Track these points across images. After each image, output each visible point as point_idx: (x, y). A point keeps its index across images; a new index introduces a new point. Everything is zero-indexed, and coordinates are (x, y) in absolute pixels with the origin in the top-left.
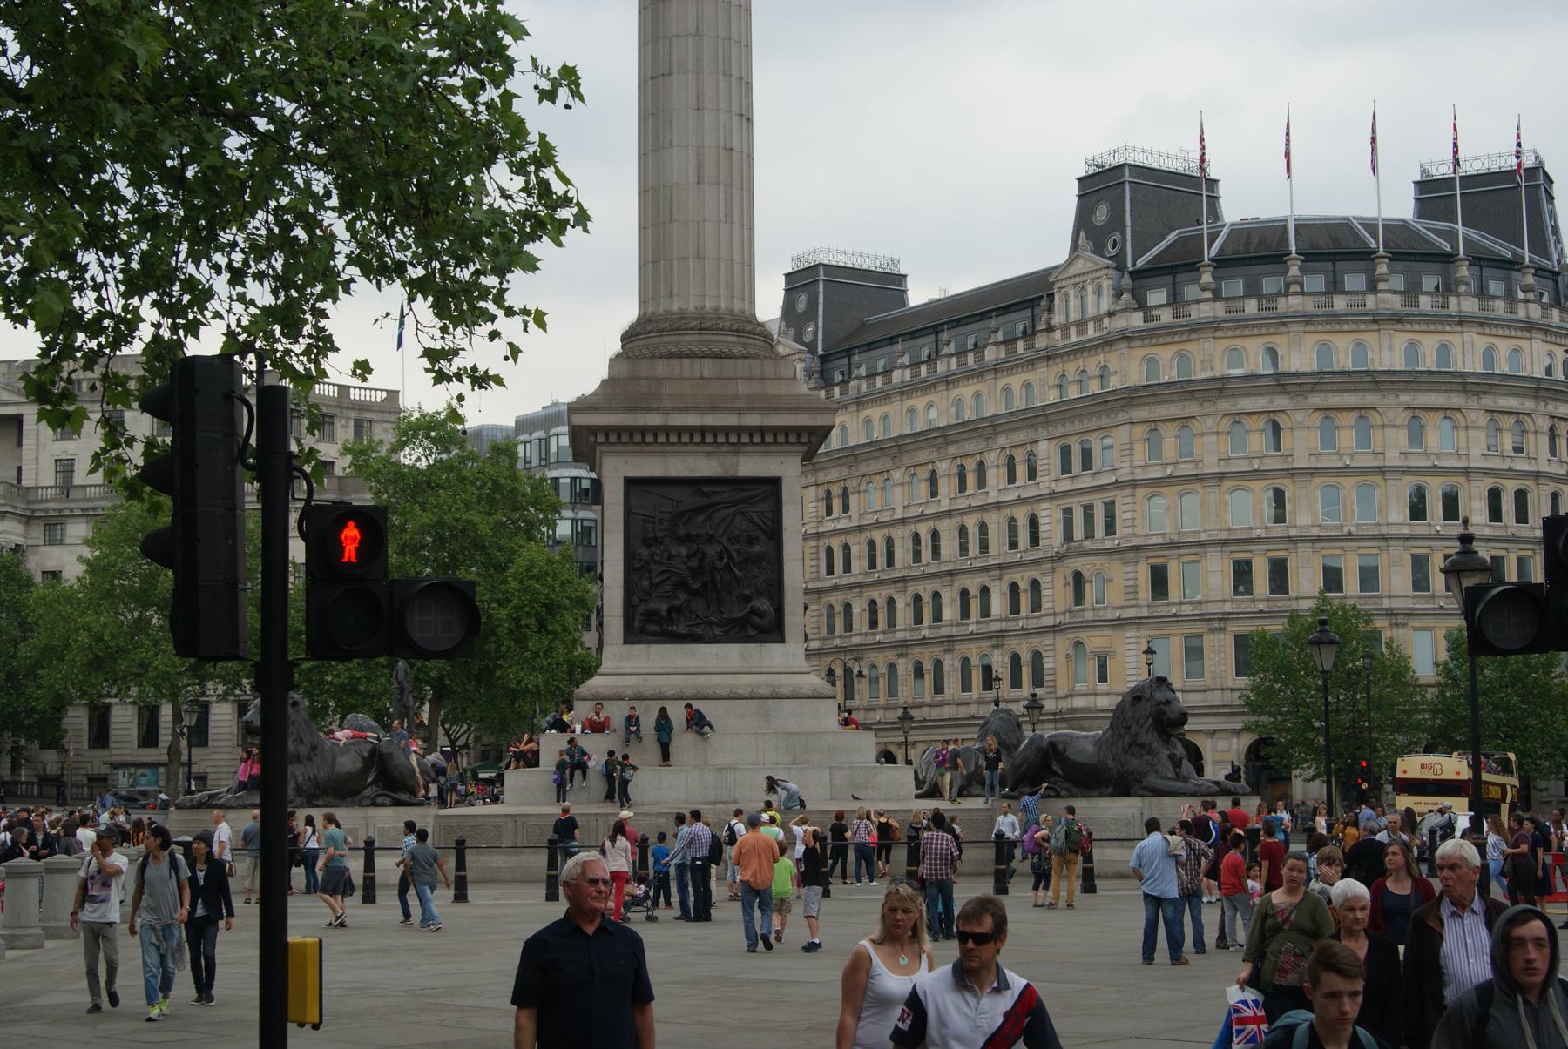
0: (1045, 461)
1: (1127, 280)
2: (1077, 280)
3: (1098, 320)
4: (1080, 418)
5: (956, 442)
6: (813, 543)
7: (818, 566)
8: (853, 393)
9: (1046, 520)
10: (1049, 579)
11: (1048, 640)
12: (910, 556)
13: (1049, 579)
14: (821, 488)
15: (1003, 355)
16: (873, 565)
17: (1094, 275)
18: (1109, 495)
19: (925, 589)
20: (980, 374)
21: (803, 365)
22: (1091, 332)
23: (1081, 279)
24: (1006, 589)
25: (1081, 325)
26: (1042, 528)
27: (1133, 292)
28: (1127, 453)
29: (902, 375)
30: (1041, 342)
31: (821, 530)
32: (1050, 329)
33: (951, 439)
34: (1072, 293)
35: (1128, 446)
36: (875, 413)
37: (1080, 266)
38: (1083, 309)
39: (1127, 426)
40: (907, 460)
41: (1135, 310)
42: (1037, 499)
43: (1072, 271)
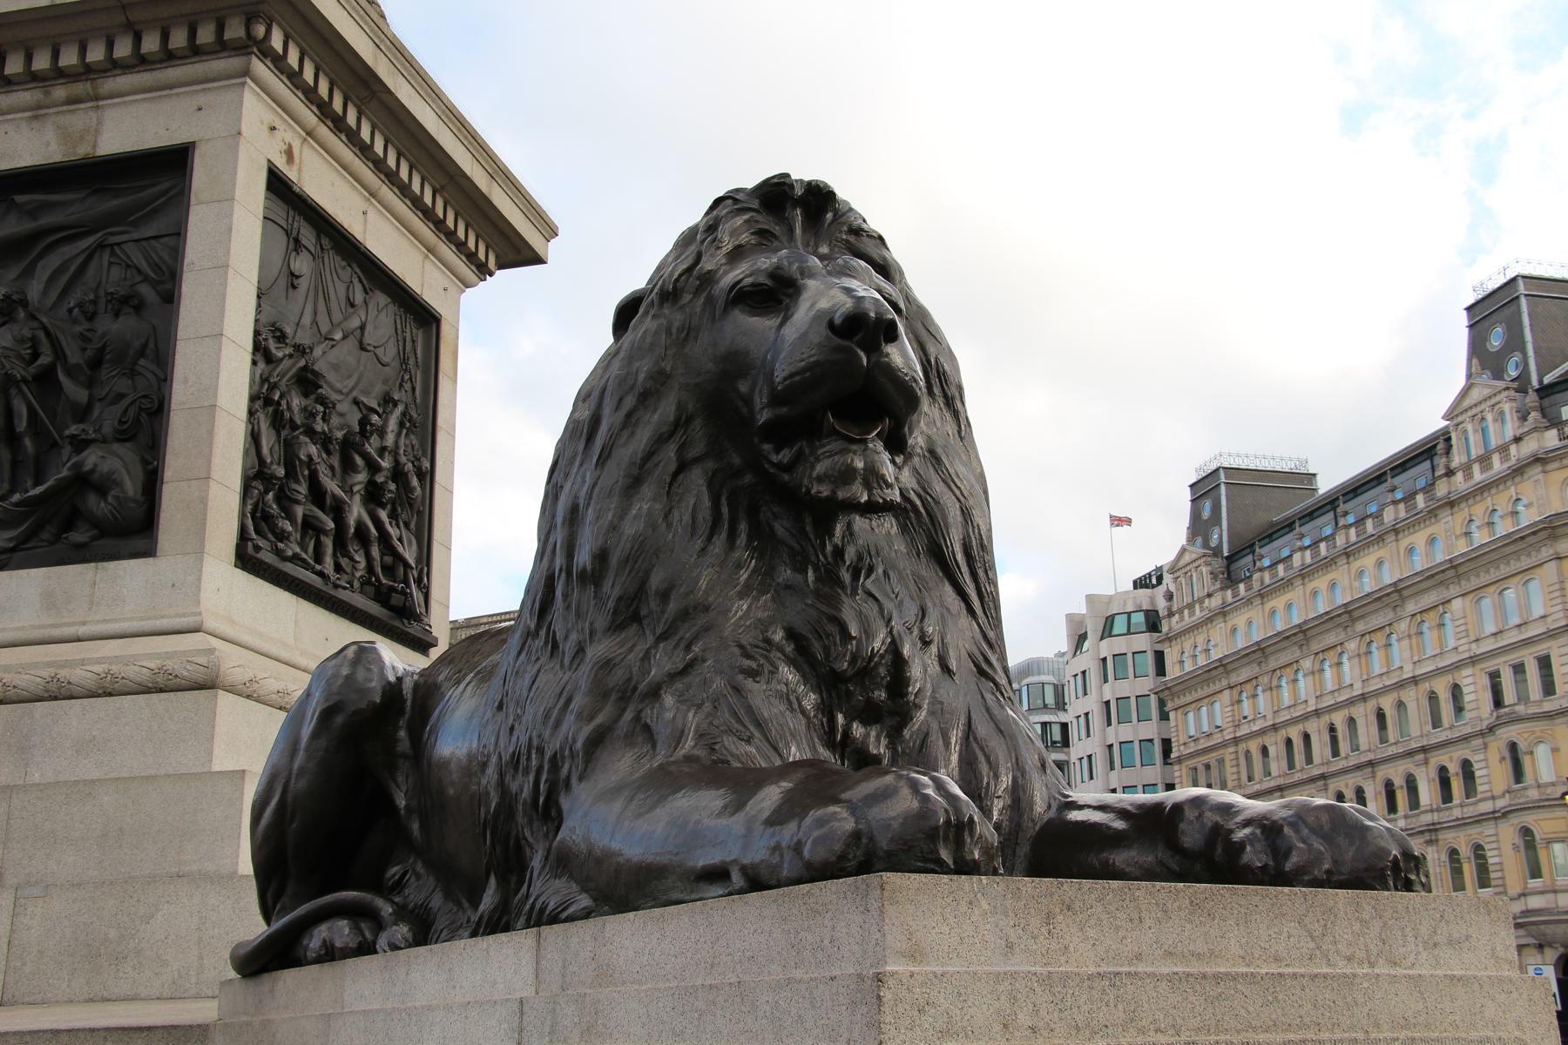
0: (1462, 621)
1: (1532, 398)
2: (1474, 411)
3: (1503, 449)
4: (1495, 563)
5: (1362, 617)
6: (1232, 749)
7: (1239, 773)
8: (1256, 586)
9: (1471, 688)
10: (1481, 757)
11: (1489, 829)
12: (1328, 751)
13: (1481, 757)
14: (1235, 690)
15: (1403, 514)
16: (1291, 765)
17: (1493, 401)
18: (1541, 649)
19: (1347, 785)
20: (1379, 539)
21: (1209, 568)
22: (1497, 465)
23: (1479, 409)
24: (1433, 774)
25: (1484, 460)
26: (1467, 698)
27: (1542, 411)
28: (1558, 594)
29: (1303, 558)
30: (1442, 489)
31: (1238, 734)
32: (1450, 473)
33: (1356, 614)
34: (1470, 427)
35: (1557, 587)
36: (1278, 602)
37: (1476, 394)
38: (1486, 442)
39: (1554, 562)
40: (1315, 646)
41: (1547, 428)
42: (1456, 667)
43: (1467, 403)
